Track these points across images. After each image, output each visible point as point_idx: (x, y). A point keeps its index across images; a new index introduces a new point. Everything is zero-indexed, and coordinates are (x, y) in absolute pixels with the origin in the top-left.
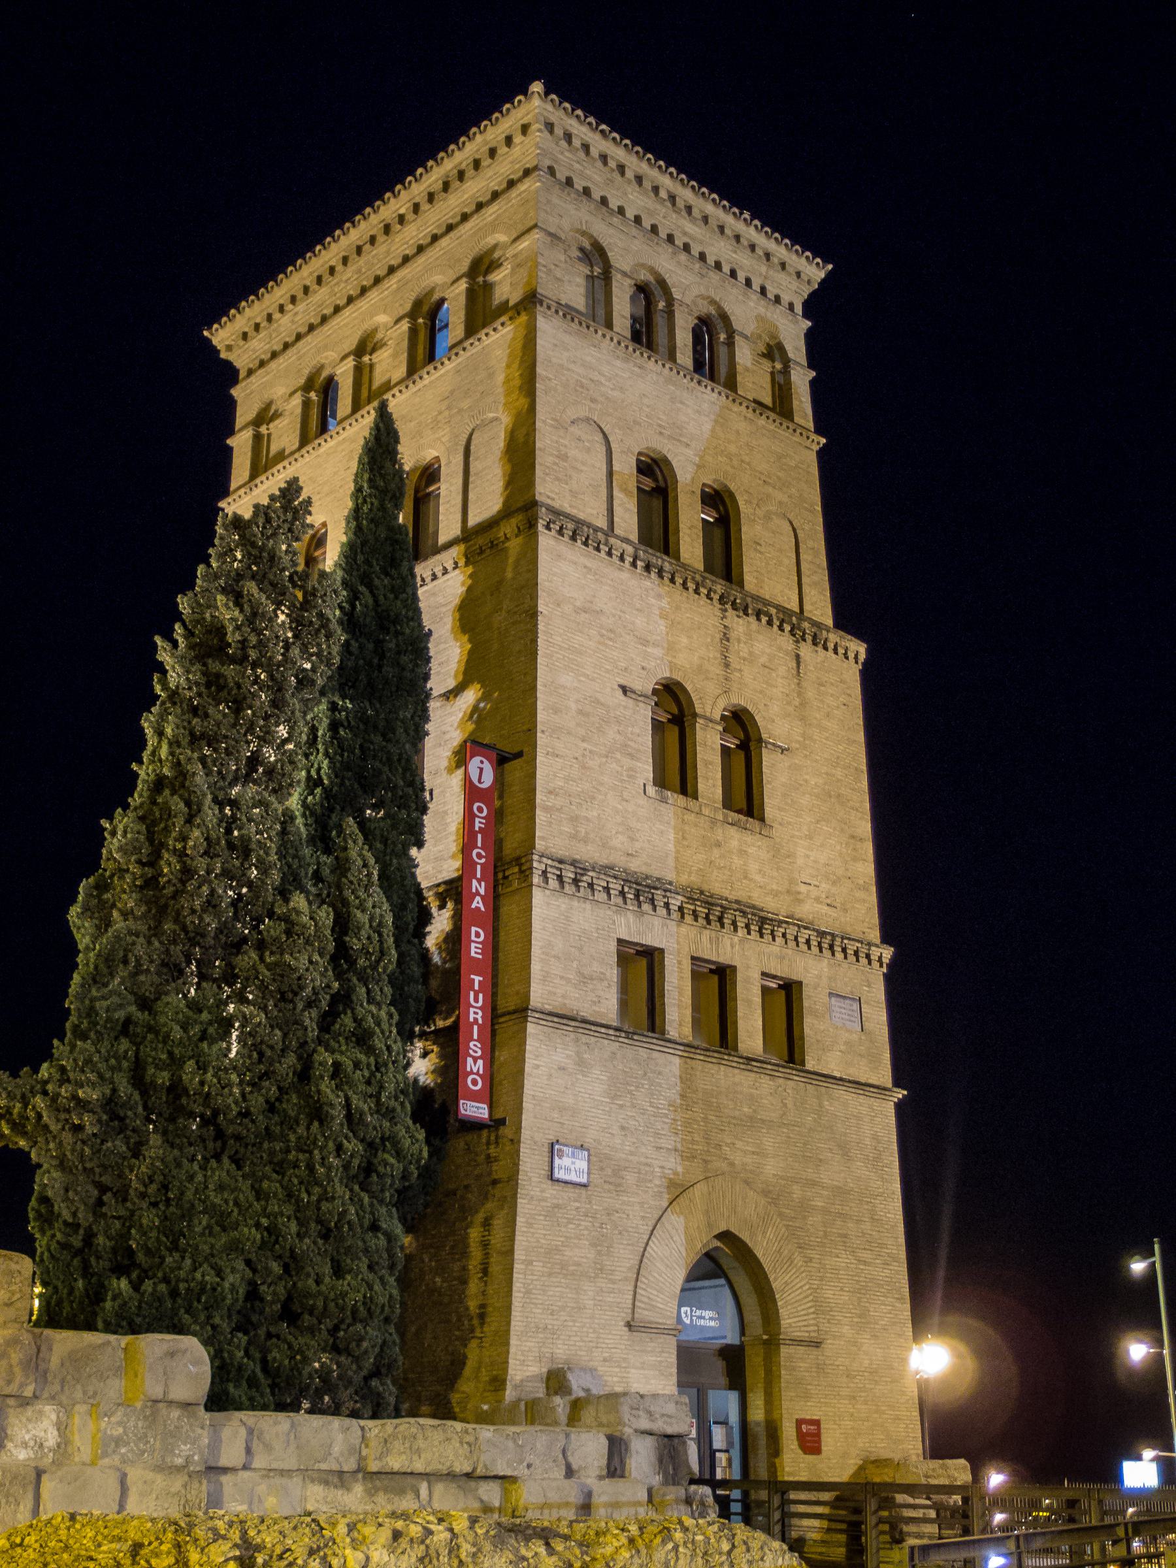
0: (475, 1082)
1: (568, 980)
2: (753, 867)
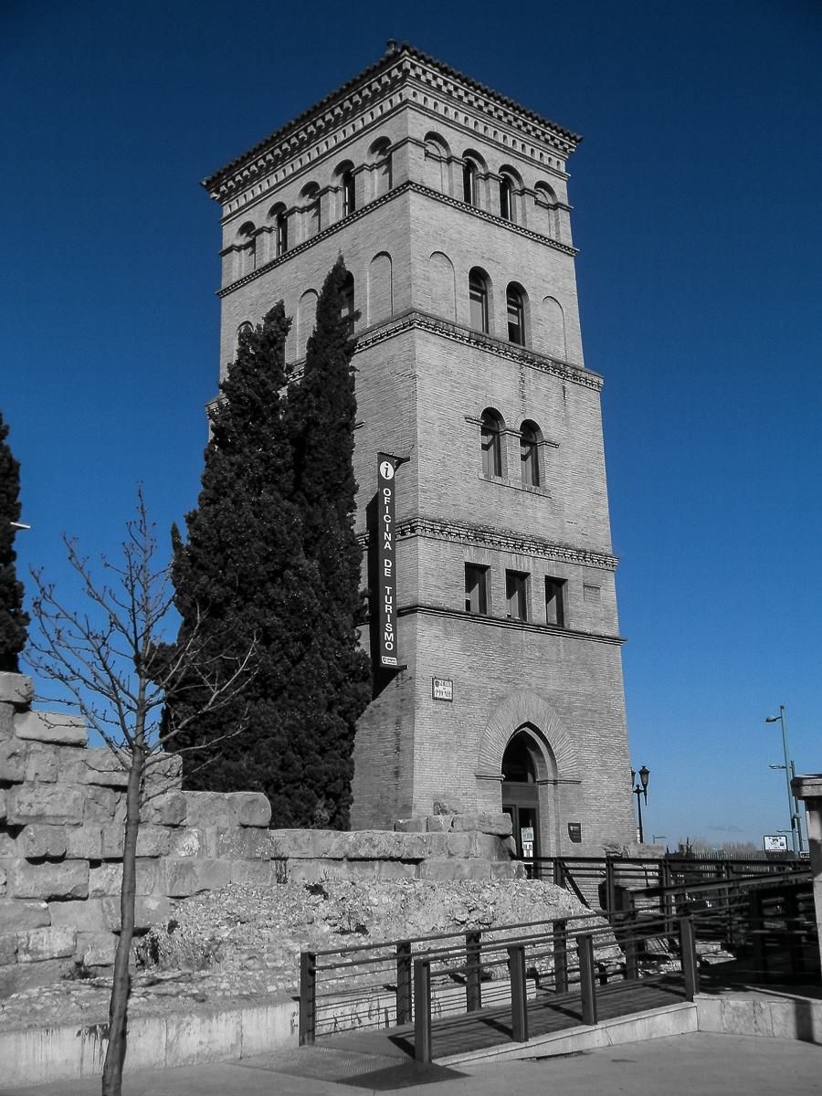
0: (389, 646)
1: (439, 588)
2: (539, 515)
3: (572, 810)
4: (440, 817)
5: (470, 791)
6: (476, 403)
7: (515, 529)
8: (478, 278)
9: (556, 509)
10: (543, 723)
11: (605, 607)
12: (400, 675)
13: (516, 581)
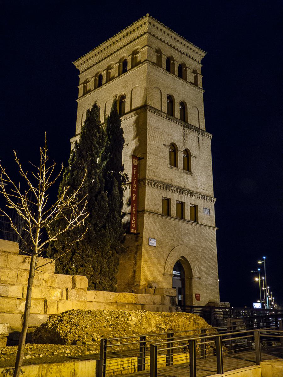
0: (134, 225)
2: (189, 182)
4: (150, 289)
9: (194, 179)
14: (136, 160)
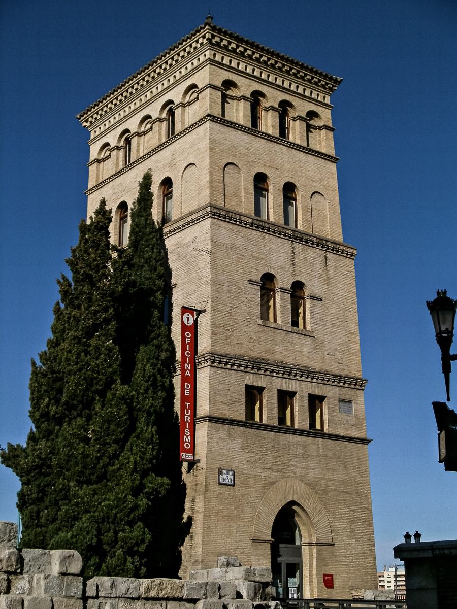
1: (225, 404)
2: (305, 349)
3: (326, 565)
5: (246, 550)
6: (257, 270)
7: (285, 360)
8: (260, 180)
10: (304, 501)
11: (356, 416)
12: (195, 467)
13: (285, 398)
14: (191, 316)
